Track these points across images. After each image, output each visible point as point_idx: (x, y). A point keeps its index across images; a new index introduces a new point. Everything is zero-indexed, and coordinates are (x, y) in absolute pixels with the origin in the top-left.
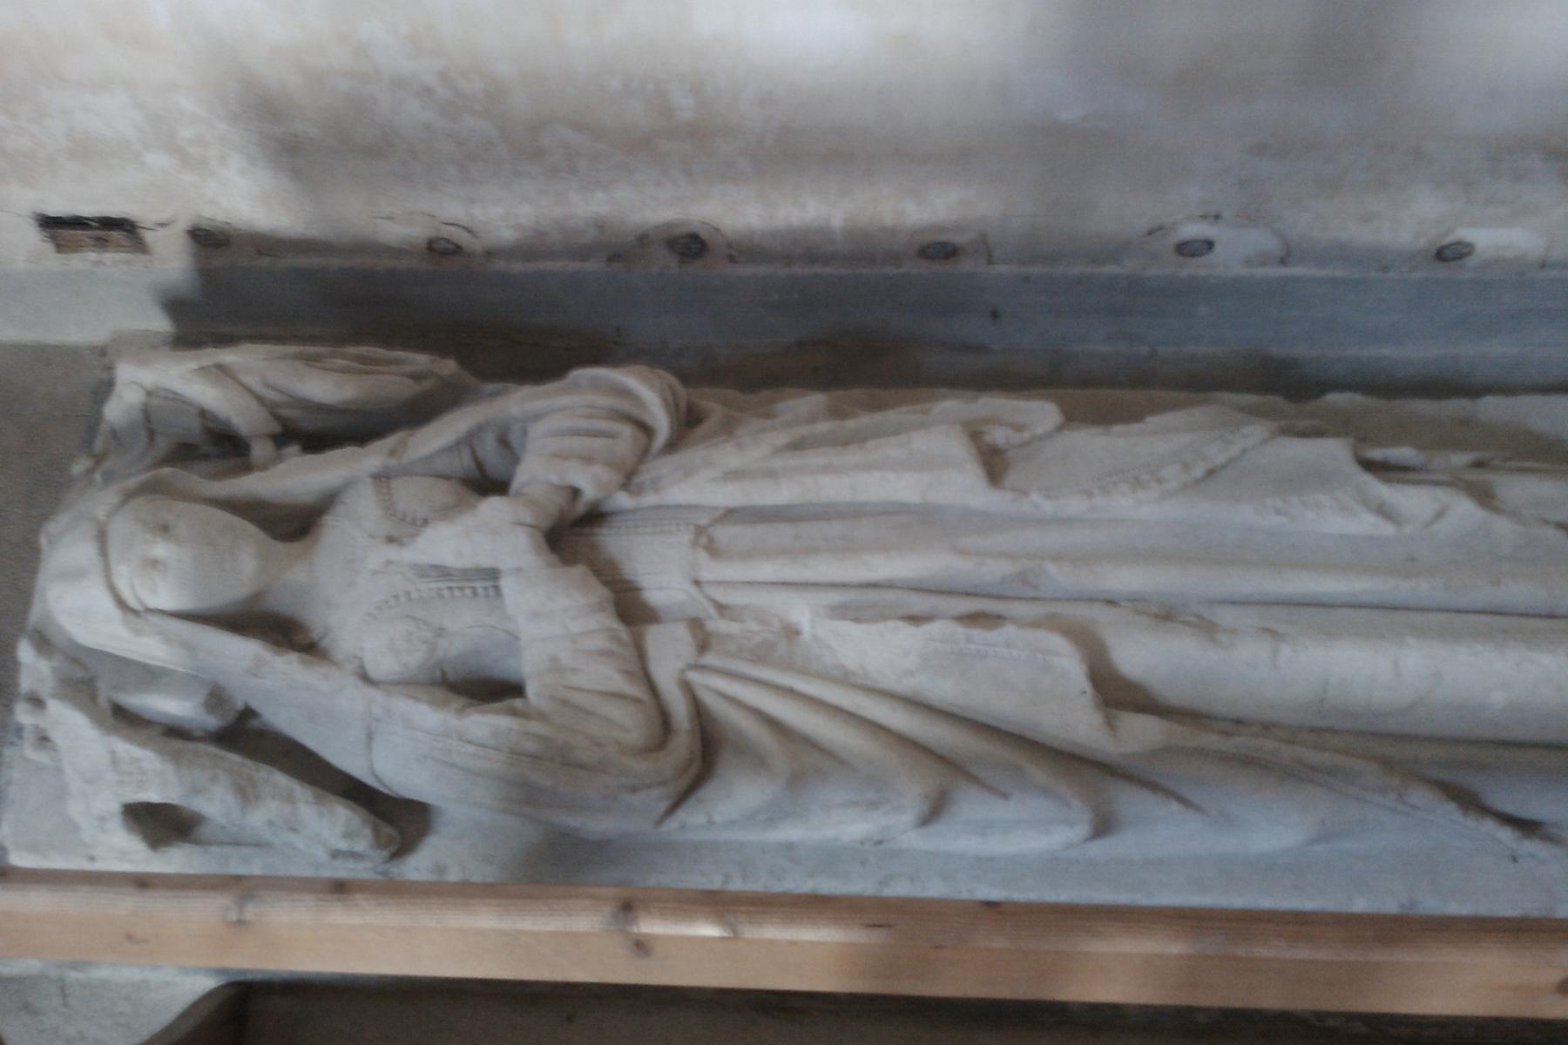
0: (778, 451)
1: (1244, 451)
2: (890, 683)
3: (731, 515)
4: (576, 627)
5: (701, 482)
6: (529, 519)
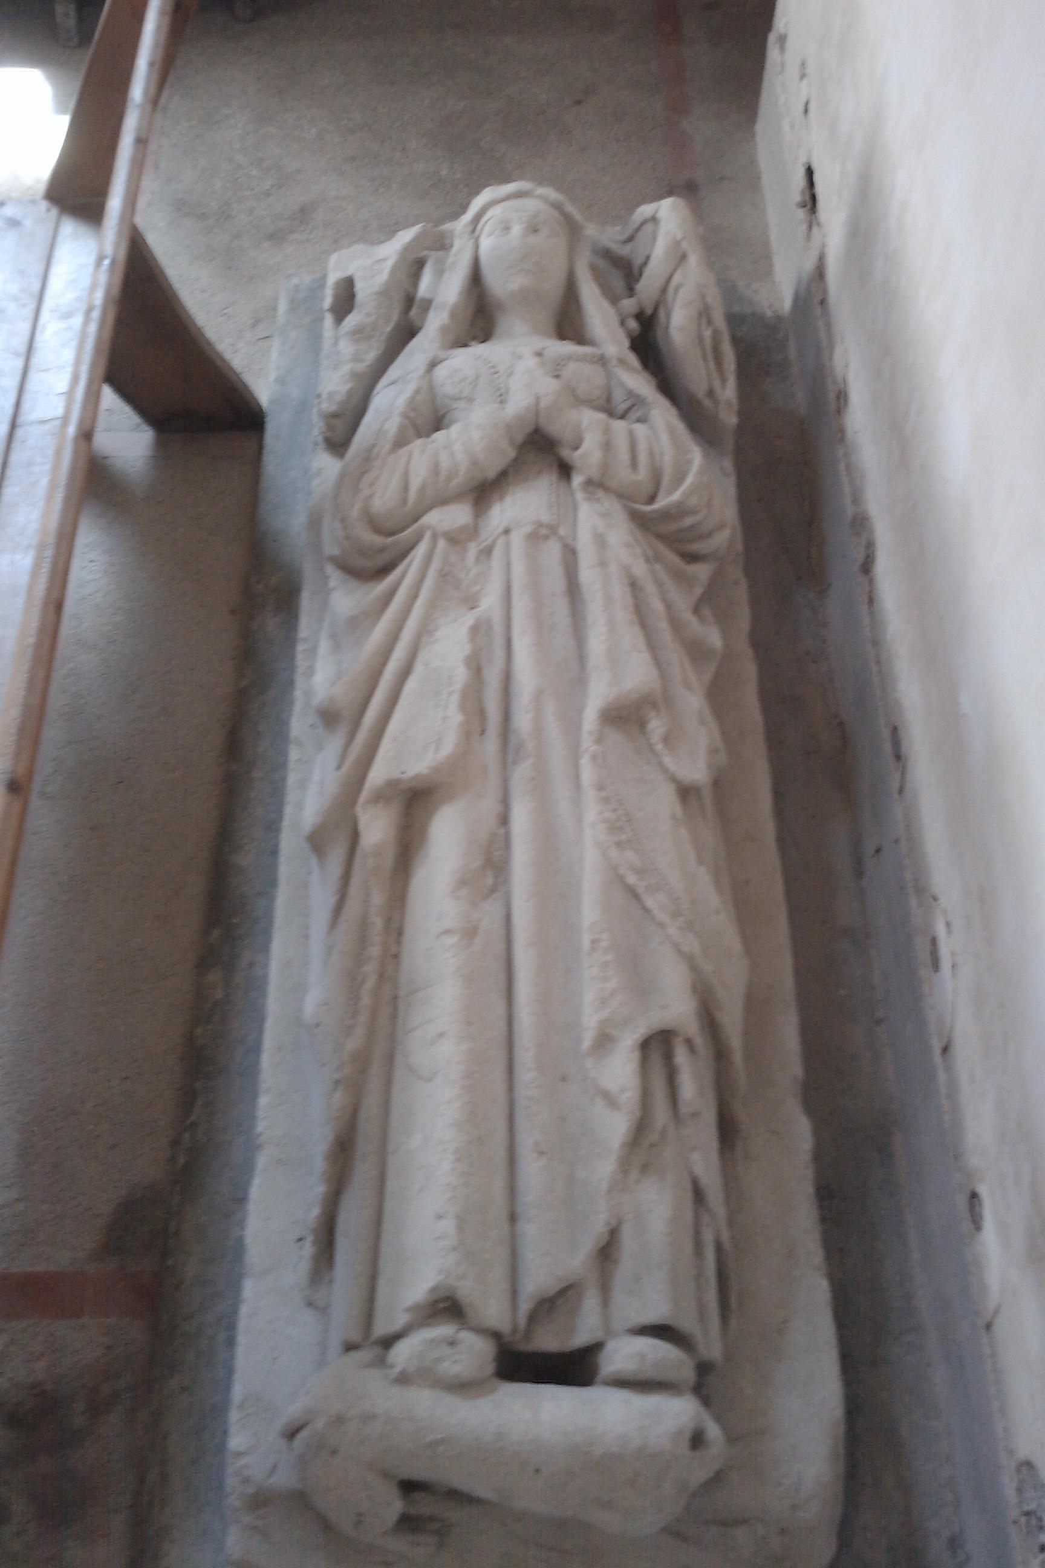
0: (627, 570)
1: (661, 925)
2: (50, 234)
3: (570, 555)
4: (457, 447)
5: (600, 532)
6: (544, 404)
